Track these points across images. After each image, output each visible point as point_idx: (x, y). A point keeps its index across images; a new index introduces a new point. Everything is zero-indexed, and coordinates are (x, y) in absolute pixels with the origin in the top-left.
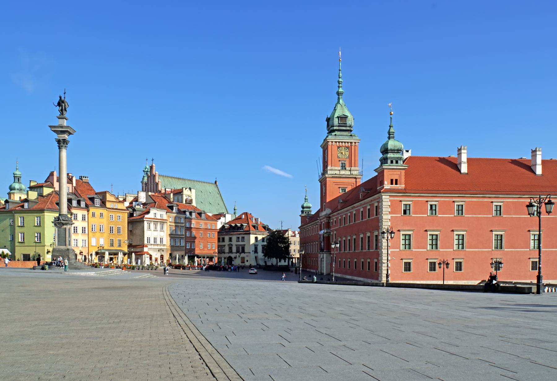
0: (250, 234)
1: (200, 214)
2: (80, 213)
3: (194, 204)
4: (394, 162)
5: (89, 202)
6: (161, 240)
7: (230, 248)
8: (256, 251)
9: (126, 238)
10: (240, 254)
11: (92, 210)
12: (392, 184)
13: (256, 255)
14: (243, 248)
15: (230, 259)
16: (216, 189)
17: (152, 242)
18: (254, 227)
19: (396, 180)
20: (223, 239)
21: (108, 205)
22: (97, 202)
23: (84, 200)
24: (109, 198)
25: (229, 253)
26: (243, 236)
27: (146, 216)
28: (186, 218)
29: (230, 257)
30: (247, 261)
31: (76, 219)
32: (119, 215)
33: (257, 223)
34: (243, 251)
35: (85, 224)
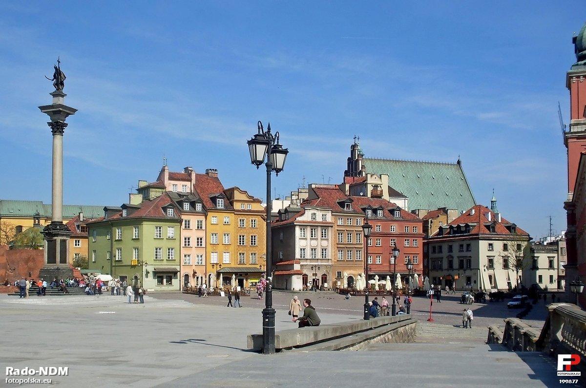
0: (478, 239)
1: (392, 212)
2: (194, 220)
3: (386, 196)
5: (209, 205)
6: (324, 250)
7: (451, 264)
10: (465, 270)
11: (210, 214)
13: (491, 272)
14: (469, 261)
16: (458, 173)
17: (308, 255)
18: (488, 227)
20: (440, 247)
21: (237, 206)
22: (221, 203)
23: (201, 201)
24: (237, 196)
25: (448, 270)
26: (468, 242)
27: (299, 219)
30: (475, 282)
31: (187, 227)
32: (254, 219)
33: (495, 222)
34: (469, 267)
35: (201, 234)
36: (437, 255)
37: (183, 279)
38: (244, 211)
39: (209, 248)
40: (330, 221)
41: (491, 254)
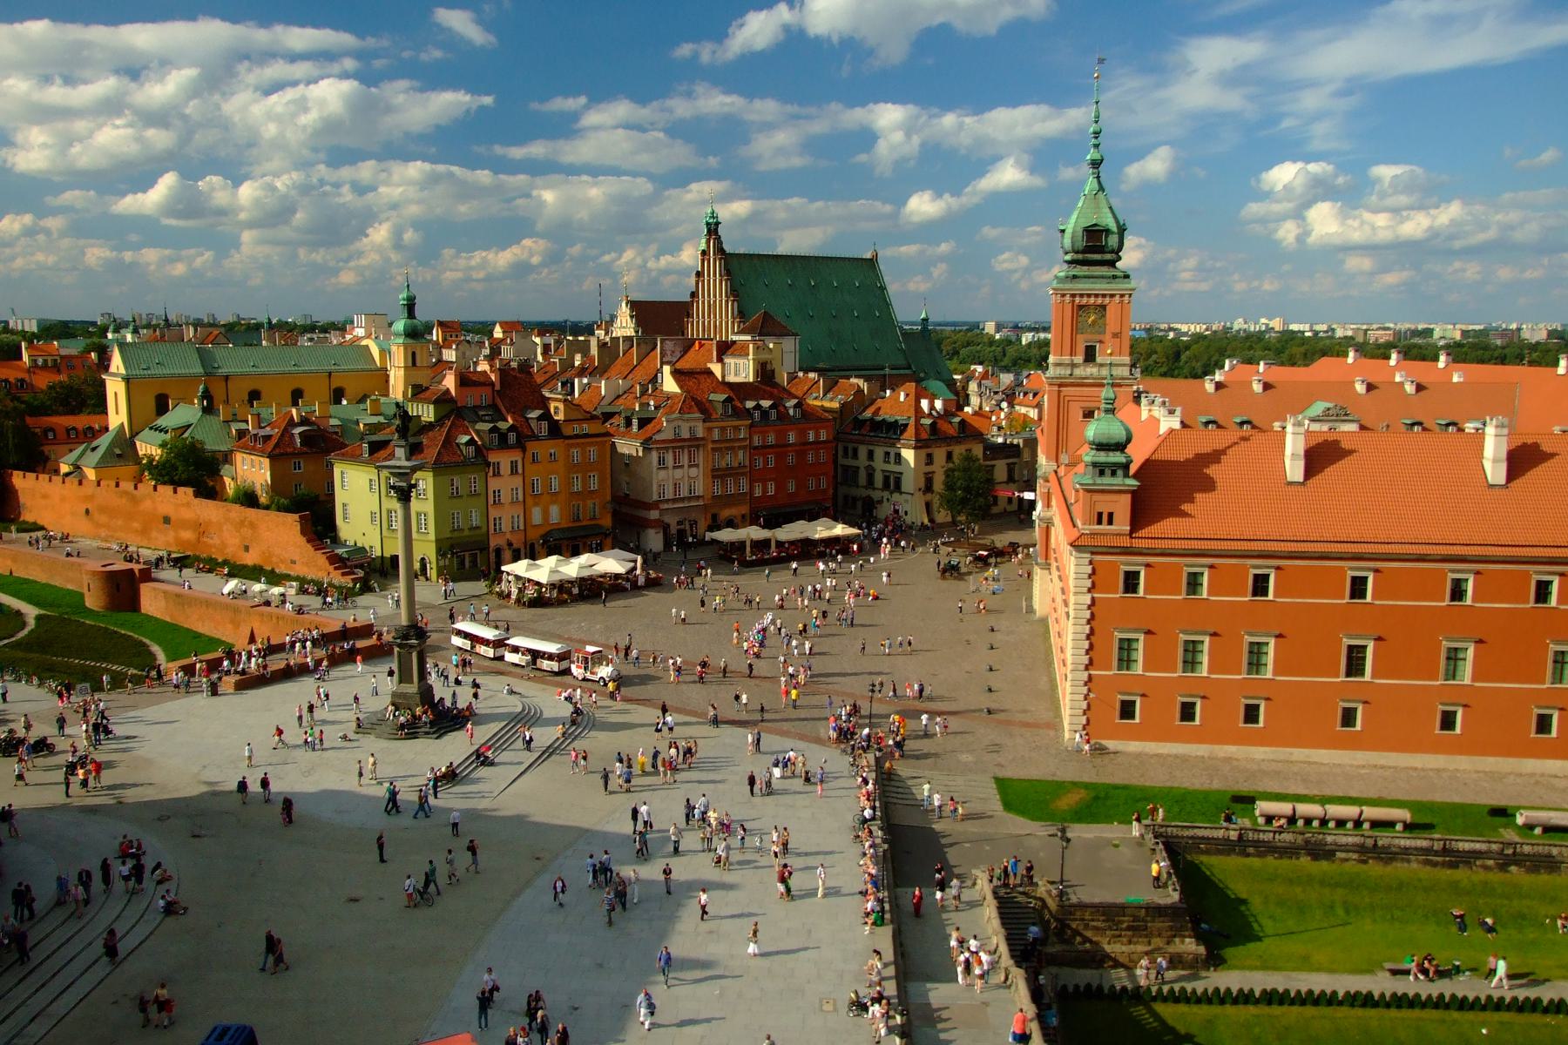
2: (504, 459)
4: (1108, 472)
8: (928, 488)
9: (609, 498)
12: (1100, 522)
13: (929, 497)
15: (870, 505)
19: (1111, 515)
20: (855, 451)
21: (567, 431)
28: (751, 426)
29: (869, 497)
31: (497, 474)
34: (898, 488)
35: (517, 481)
36: (850, 462)
37: (492, 556)
38: (577, 436)
39: (529, 501)
40: (700, 434)
41: (929, 469)
